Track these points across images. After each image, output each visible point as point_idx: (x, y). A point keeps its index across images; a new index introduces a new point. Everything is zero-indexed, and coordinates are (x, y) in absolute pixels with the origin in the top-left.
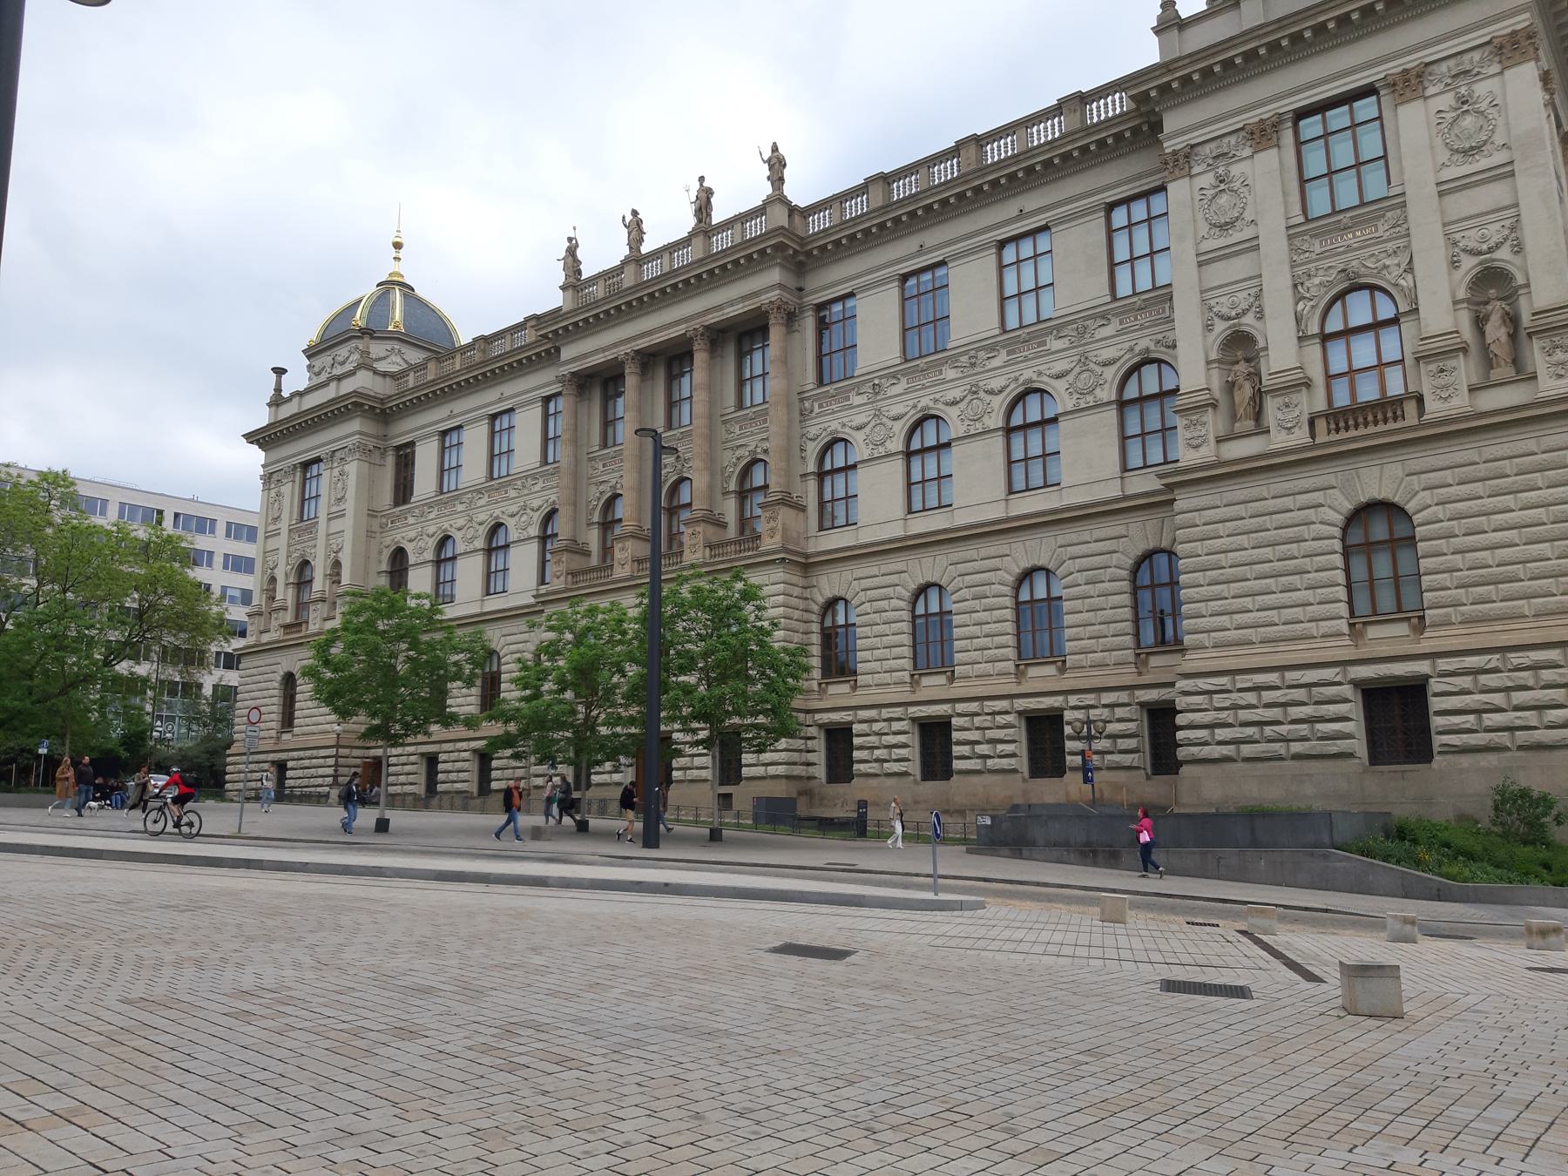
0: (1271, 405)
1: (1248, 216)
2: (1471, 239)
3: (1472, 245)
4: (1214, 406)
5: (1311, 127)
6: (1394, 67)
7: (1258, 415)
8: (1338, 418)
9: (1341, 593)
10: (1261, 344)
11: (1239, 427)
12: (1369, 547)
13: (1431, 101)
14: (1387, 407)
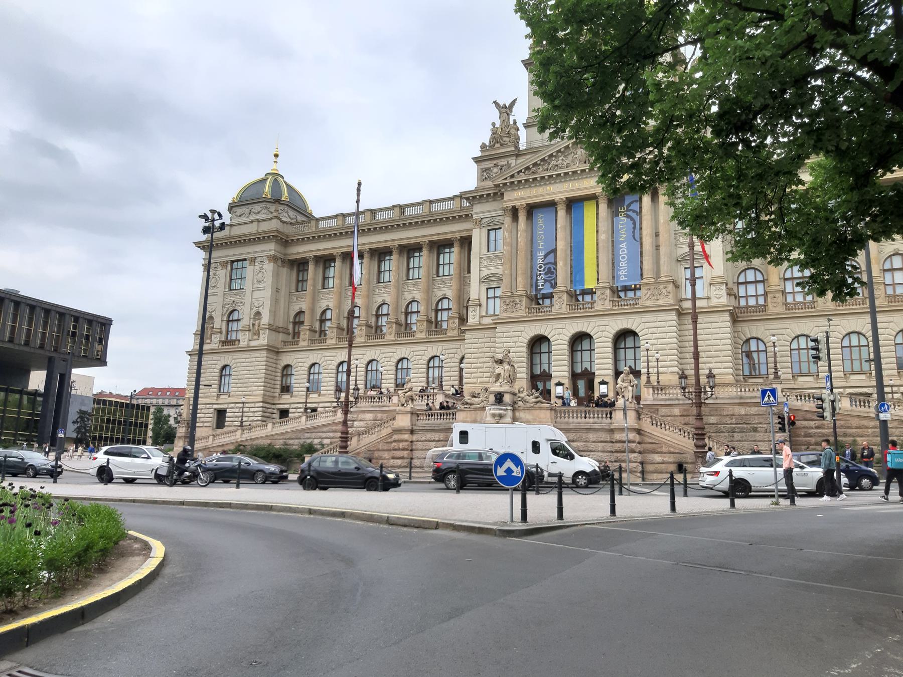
6: (250, 256)
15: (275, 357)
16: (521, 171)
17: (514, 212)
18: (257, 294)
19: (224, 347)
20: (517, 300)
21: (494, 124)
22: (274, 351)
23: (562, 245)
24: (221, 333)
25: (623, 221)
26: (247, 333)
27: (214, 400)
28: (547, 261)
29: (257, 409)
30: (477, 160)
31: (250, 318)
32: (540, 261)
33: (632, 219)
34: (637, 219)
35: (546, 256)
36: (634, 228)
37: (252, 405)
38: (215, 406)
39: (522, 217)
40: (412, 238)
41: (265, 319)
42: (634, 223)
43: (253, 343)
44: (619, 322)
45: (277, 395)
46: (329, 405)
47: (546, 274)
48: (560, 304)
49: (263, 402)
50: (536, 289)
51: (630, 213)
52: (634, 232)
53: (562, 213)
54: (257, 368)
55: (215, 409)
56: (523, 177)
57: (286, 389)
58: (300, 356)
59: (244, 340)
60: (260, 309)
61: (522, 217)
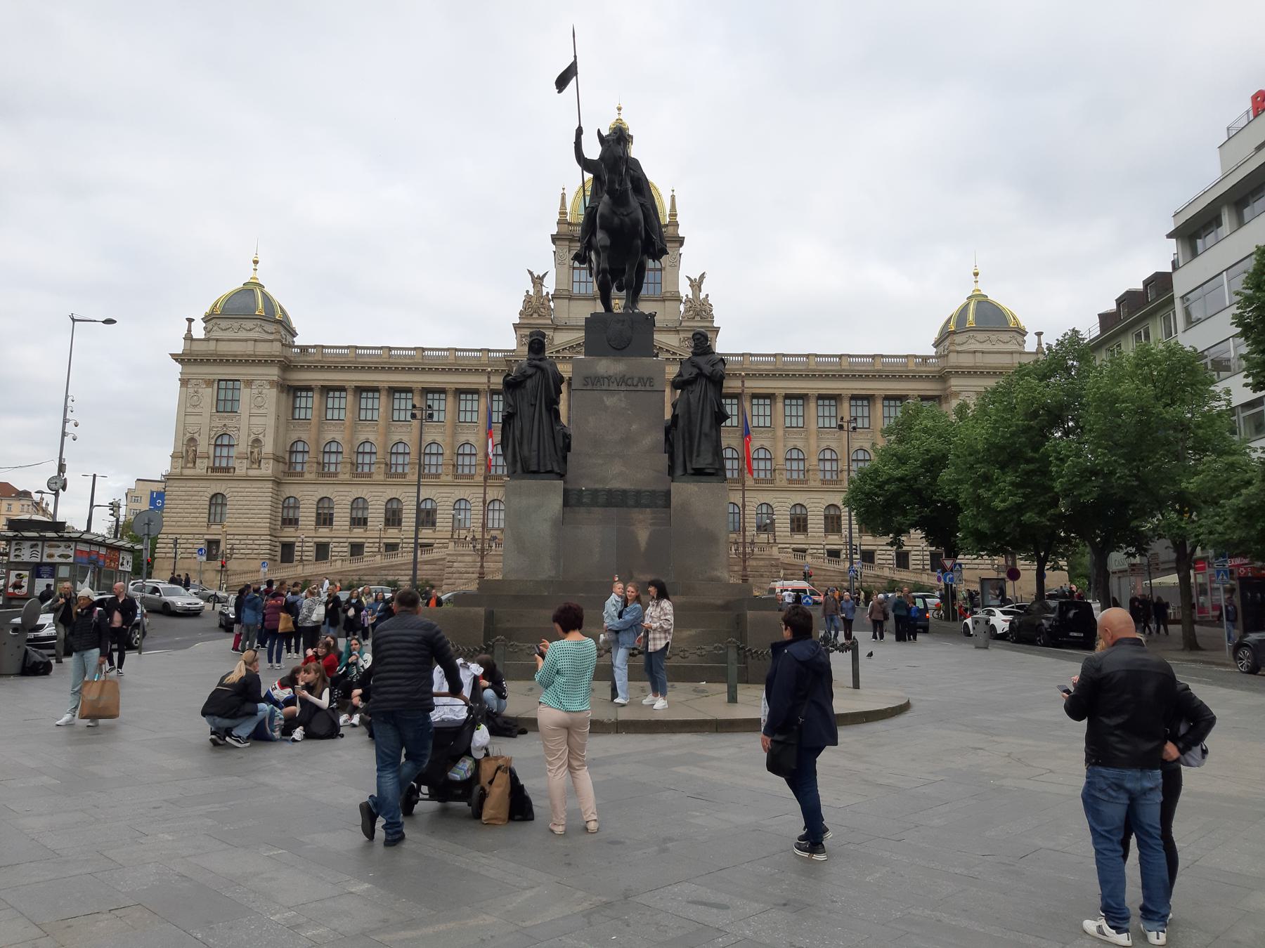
0: (198, 461)
1: (201, 405)
2: (255, 430)
3: (255, 432)
4: (182, 458)
5: (223, 384)
7: (195, 463)
8: (214, 469)
9: (206, 515)
10: (198, 443)
11: (189, 465)
12: (216, 504)
13: (253, 390)
14: (227, 469)
15: (277, 489)
16: (566, 348)
18: (254, 420)
19: (215, 474)
21: (527, 292)
22: (278, 483)
24: (208, 458)
26: (245, 461)
27: (204, 530)
29: (264, 541)
30: (516, 327)
31: (248, 445)
37: (257, 537)
38: (206, 537)
40: (437, 383)
41: (268, 447)
43: (252, 473)
45: (279, 527)
46: (344, 540)
49: (269, 535)
54: (259, 499)
55: (206, 540)
57: (292, 522)
58: (305, 489)
59: (241, 468)
60: (260, 436)
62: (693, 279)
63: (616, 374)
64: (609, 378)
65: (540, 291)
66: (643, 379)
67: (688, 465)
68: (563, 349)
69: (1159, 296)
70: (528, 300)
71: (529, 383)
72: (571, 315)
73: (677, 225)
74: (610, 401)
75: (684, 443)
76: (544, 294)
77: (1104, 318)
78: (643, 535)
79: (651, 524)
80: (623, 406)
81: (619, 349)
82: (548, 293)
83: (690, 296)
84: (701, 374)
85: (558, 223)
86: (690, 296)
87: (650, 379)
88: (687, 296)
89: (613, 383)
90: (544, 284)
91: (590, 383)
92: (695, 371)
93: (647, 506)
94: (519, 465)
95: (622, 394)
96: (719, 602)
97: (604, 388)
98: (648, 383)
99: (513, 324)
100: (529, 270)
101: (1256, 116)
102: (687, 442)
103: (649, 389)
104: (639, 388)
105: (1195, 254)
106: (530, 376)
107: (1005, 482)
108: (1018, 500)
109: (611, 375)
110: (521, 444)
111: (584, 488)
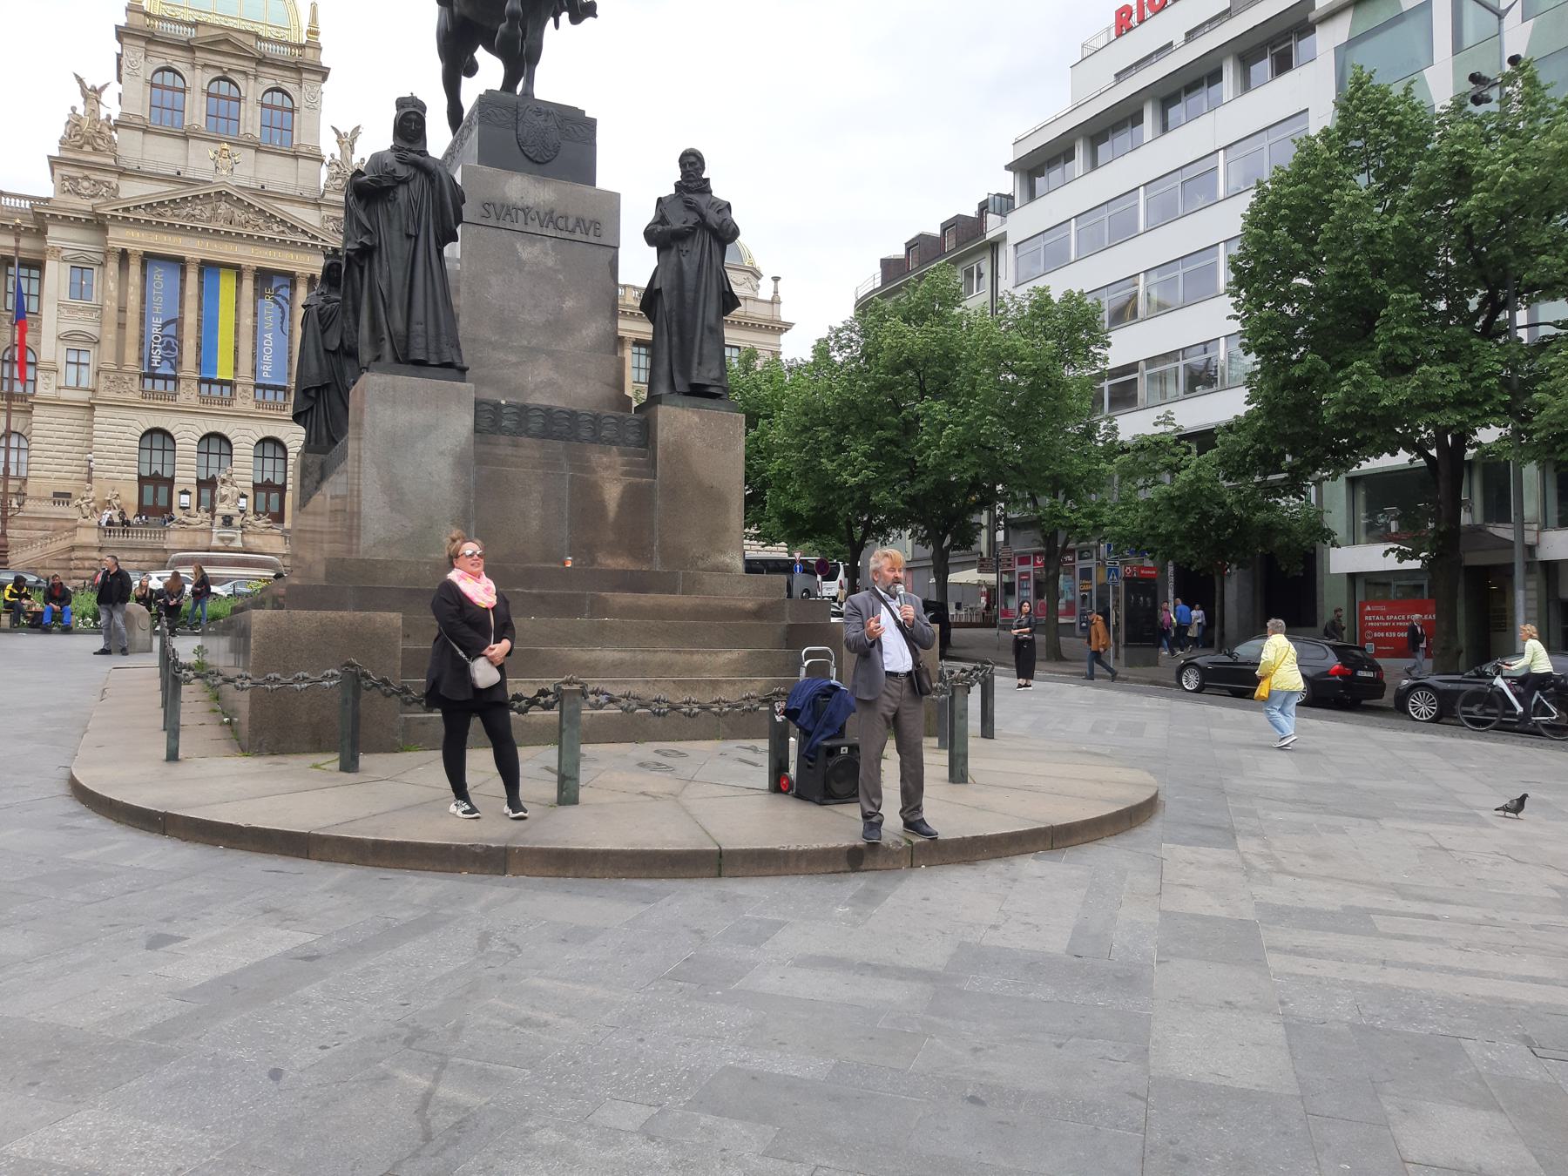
16: (140, 206)
17: (124, 256)
20: (127, 378)
21: (73, 109)
23: (190, 318)
25: (267, 305)
28: (166, 331)
32: (155, 331)
33: (281, 307)
34: (287, 308)
35: (164, 325)
36: (283, 318)
39: (135, 268)
42: (283, 312)
44: (265, 428)
47: (163, 349)
48: (188, 394)
50: (150, 367)
51: (279, 299)
52: (282, 323)
53: (192, 277)
56: (142, 215)
61: (135, 268)
62: (342, 131)
63: (539, 204)
64: (526, 210)
65: (94, 112)
66: (583, 221)
67: (678, 379)
68: (135, 207)
69: (959, 245)
70: (74, 124)
71: (402, 194)
72: (146, 157)
73: (318, 48)
74: (528, 252)
75: (670, 340)
76: (103, 116)
77: (888, 266)
78: (612, 493)
79: (625, 474)
80: (550, 263)
81: (537, 162)
82: (109, 118)
83: (338, 157)
84: (703, 224)
85: (127, 10)
86: (338, 157)
87: (596, 223)
88: (332, 156)
89: (532, 220)
90: (102, 100)
91: (493, 214)
92: (693, 218)
93: (612, 442)
94: (387, 346)
95: (549, 243)
96: (750, 605)
97: (516, 226)
98: (592, 228)
99: (49, 157)
100: (76, 76)
101: (1119, 35)
102: (675, 339)
103: (594, 240)
104: (578, 236)
105: (1032, 196)
106: (405, 181)
107: (857, 450)
108: (872, 475)
109: (531, 205)
110: (388, 308)
111: (503, 402)
